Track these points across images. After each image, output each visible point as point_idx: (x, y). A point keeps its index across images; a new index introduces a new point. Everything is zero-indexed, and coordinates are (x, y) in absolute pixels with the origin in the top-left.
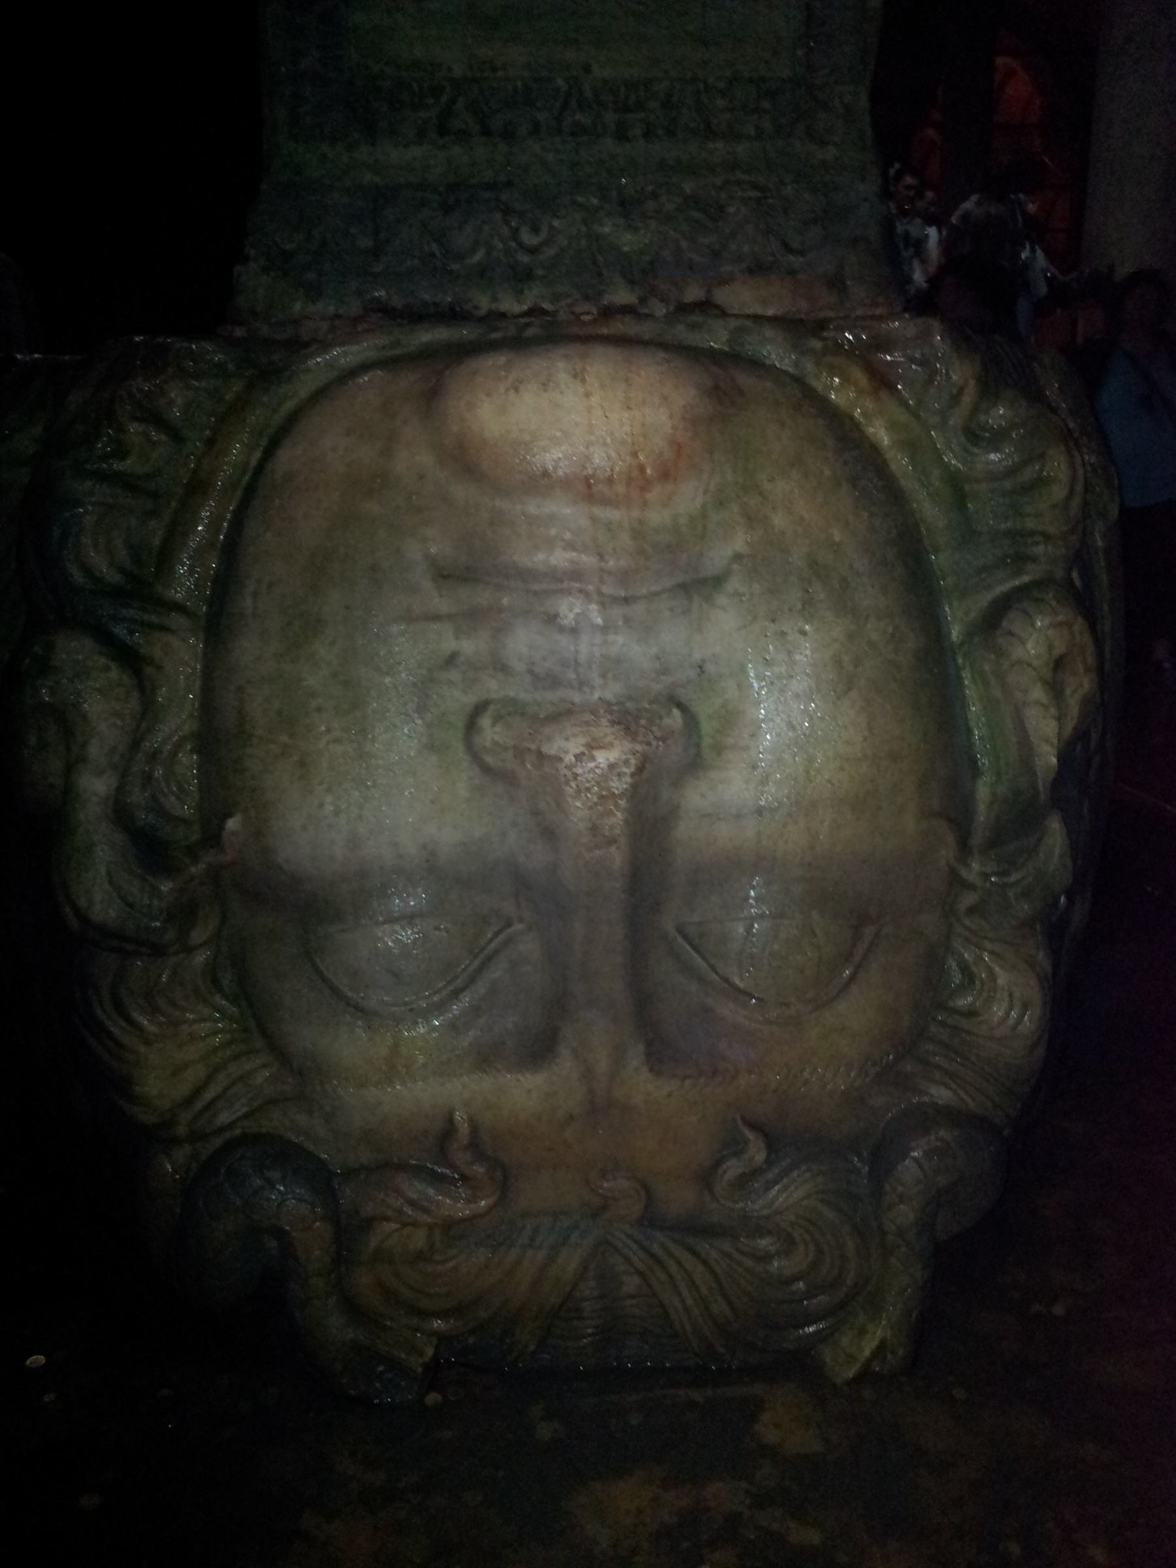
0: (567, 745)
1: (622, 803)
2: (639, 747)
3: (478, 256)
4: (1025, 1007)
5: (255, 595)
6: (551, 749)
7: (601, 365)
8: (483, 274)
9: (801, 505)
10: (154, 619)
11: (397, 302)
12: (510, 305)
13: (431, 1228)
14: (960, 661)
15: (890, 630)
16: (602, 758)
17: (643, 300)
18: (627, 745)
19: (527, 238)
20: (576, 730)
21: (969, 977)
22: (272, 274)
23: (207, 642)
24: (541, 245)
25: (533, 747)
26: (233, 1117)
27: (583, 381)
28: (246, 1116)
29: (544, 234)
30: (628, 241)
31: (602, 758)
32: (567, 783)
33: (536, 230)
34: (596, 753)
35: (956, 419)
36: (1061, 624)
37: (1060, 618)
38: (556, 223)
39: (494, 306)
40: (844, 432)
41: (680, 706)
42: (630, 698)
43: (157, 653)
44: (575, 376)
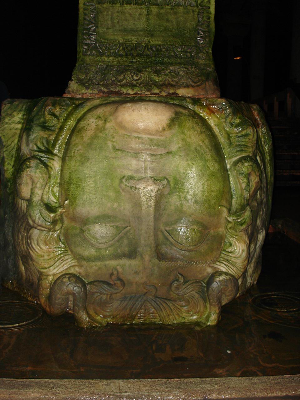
0: (141, 186)
1: (153, 198)
2: (157, 187)
4: (243, 251)
5: (74, 153)
6: (138, 186)
7: (151, 106)
8: (126, 85)
9: (195, 137)
10: (51, 157)
11: (106, 90)
12: (131, 92)
13: (107, 295)
14: (229, 173)
15: (212, 164)
16: (150, 188)
17: (160, 92)
18: (155, 186)
19: (135, 78)
21: (231, 245)
22: (78, 84)
24: (138, 79)
25: (134, 186)
26: (63, 270)
27: (147, 110)
28: (67, 269)
29: (139, 77)
30: (157, 79)
31: (150, 188)
32: (141, 193)
33: (137, 76)
34: (148, 187)
35: (228, 121)
36: (250, 165)
37: (250, 164)
38: (142, 75)
39: (127, 92)
40: (204, 122)
41: (167, 179)
42: (156, 177)
44: (146, 109)
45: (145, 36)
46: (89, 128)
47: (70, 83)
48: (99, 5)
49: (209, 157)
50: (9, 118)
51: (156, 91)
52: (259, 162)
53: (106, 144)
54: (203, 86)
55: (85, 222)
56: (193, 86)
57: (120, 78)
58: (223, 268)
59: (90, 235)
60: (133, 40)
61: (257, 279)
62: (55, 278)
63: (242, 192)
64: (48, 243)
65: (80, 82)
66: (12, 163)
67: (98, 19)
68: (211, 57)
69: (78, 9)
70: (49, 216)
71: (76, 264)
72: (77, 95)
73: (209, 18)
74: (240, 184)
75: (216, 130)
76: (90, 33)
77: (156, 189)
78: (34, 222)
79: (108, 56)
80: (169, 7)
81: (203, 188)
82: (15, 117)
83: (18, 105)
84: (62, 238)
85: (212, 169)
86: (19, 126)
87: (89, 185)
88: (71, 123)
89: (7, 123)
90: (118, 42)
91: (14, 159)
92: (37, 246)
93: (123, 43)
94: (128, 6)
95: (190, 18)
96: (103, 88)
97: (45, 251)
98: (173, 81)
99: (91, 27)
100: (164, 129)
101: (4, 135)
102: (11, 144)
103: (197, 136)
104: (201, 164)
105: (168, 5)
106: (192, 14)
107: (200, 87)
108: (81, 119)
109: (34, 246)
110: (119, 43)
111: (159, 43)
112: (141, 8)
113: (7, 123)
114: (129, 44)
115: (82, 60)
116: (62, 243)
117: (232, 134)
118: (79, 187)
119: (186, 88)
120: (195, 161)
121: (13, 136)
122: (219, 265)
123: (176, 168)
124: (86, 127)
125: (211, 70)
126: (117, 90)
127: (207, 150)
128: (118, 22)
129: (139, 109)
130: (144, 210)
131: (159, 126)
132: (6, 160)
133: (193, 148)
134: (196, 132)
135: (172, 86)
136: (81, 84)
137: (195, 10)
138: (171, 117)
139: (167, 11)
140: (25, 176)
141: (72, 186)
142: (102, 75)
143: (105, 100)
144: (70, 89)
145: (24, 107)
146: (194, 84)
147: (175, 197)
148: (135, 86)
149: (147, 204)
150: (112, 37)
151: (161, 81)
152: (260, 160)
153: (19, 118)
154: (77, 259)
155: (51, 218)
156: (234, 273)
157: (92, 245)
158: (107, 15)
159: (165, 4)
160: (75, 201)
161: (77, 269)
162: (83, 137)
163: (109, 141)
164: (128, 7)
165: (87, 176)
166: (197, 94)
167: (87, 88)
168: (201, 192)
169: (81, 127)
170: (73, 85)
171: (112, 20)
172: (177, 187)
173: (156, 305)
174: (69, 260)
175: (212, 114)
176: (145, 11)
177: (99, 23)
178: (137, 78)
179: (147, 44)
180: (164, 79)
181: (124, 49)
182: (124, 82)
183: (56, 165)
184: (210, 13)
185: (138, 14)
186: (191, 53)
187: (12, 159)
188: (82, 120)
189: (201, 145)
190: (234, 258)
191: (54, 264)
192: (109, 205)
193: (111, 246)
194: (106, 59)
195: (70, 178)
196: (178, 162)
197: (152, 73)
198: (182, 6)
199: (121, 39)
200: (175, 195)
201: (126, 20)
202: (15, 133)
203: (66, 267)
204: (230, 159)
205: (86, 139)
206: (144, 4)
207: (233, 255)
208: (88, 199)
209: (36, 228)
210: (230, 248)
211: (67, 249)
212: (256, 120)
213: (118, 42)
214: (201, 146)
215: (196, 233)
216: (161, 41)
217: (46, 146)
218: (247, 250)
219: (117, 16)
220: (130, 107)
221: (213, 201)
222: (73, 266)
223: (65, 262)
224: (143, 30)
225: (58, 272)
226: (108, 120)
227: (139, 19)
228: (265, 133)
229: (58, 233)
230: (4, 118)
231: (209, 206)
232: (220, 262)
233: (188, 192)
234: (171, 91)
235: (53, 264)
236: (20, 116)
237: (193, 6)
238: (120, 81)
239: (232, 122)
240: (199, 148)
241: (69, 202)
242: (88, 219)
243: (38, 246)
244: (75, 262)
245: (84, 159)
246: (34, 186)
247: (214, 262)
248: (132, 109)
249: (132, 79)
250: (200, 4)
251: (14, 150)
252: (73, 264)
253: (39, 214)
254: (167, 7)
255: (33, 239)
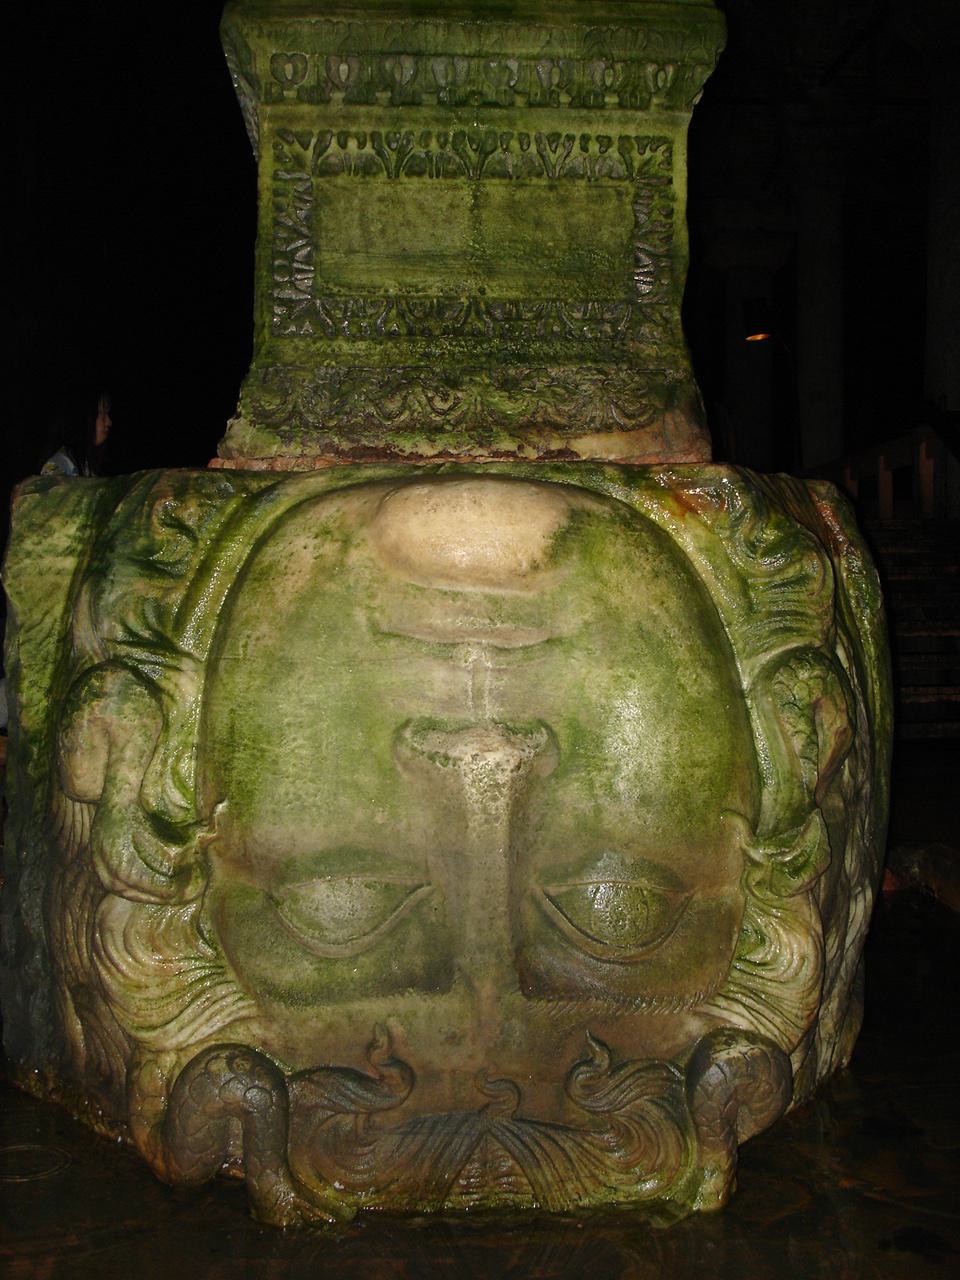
0: (464, 750)
1: (505, 791)
2: (516, 752)
3: (405, 416)
4: (803, 958)
5: (245, 646)
6: (453, 753)
8: (410, 429)
9: (635, 590)
10: (171, 662)
11: (345, 445)
12: (426, 450)
13: (356, 1114)
14: (749, 702)
16: (492, 758)
17: (520, 448)
18: (509, 750)
19: (439, 404)
20: (472, 739)
23: (206, 679)
24: (450, 409)
25: (442, 751)
26: (210, 1031)
27: (480, 505)
28: (222, 1030)
30: (509, 407)
31: (492, 758)
32: (465, 775)
33: (445, 400)
34: (487, 754)
35: (740, 535)
36: (816, 677)
37: (816, 673)
38: (460, 395)
39: (414, 450)
40: (661, 539)
41: (548, 727)
42: (512, 720)
45: (469, 273)
46: (294, 566)
47: (232, 426)
48: (320, 179)
49: (681, 652)
50: (35, 538)
51: (507, 444)
52: (845, 665)
53: (349, 615)
54: (655, 427)
55: (280, 872)
56: (623, 429)
57: (392, 406)
58: (740, 1019)
59: (299, 913)
60: (430, 287)
61: (849, 1049)
62: (185, 1061)
63: (792, 765)
64: (160, 942)
65: (265, 420)
66: (46, 682)
67: (319, 221)
68: (680, 334)
69: (254, 194)
70: (165, 854)
71: (253, 1011)
72: (255, 462)
73: (670, 214)
74: (787, 740)
75: (701, 564)
76: (295, 265)
77: (512, 761)
78: (114, 874)
79: (353, 339)
80: (544, 182)
81: (666, 755)
82: (56, 535)
83: (65, 497)
84: (206, 926)
85: (693, 691)
86: (70, 563)
87: (294, 751)
88: (236, 550)
89: (28, 554)
90: (382, 292)
91: (50, 668)
92: (125, 954)
93: (398, 297)
94: (415, 179)
95: (610, 215)
96: (336, 440)
97: (151, 971)
98: (559, 412)
99: (297, 249)
100: (535, 567)
101: (19, 593)
102: (42, 620)
103: (643, 587)
104: (656, 677)
105: (539, 175)
106: (614, 202)
107: (648, 429)
108: (269, 537)
109: (115, 955)
110: (387, 298)
111: (513, 294)
112: (456, 188)
113: (28, 554)
114: (419, 298)
115: (269, 352)
116: (206, 941)
117: (754, 576)
118: (262, 756)
119: (602, 435)
120: (637, 667)
121: (49, 595)
122: (725, 1009)
123: (575, 692)
124: (284, 563)
125: (680, 375)
126: (382, 445)
127: (674, 631)
128: (383, 232)
129: (453, 503)
130: (474, 829)
131: (519, 556)
132: (25, 671)
133: (628, 624)
134: (638, 574)
136: (268, 426)
137: (623, 190)
138: (556, 526)
139: (536, 194)
140: (85, 723)
141: (237, 755)
142: (331, 400)
143: (345, 477)
144: (232, 444)
145: (85, 500)
146: (627, 421)
147: (576, 785)
148: (439, 429)
149: (485, 810)
150: (365, 279)
152: (848, 658)
153: (69, 537)
154: (255, 996)
155: (169, 860)
156: (777, 1033)
157: (307, 949)
158: (346, 210)
159: (529, 173)
160: (249, 804)
161: (256, 1029)
162: (274, 594)
163: (358, 609)
164: (414, 183)
165: (286, 720)
166: (637, 453)
167: (287, 439)
168: (659, 769)
169: (266, 564)
170: (241, 431)
171: (364, 224)
172: (582, 751)
173: (521, 1147)
174: (230, 1000)
175: (687, 515)
176: (466, 196)
177: (323, 234)
178: (446, 406)
179: (474, 298)
180: (532, 408)
181: (401, 315)
182: (402, 418)
183: (187, 687)
184: (673, 199)
185: (444, 206)
186: (614, 323)
187: (45, 667)
188: (271, 542)
189: (658, 616)
190: (775, 984)
191: (181, 1012)
192: (360, 815)
193: (368, 950)
194: (346, 347)
195: (232, 727)
196: (583, 670)
197: (492, 389)
198: (582, 177)
199: (392, 282)
200: (577, 780)
201: (408, 224)
202: (56, 586)
203: (218, 1022)
204: (749, 656)
205: (283, 602)
206: (463, 174)
207: (769, 975)
208: (291, 796)
209: (120, 894)
210: (760, 949)
211: (225, 962)
212: (828, 529)
213: (382, 292)
214: (655, 619)
215: (645, 903)
216: (517, 289)
217: (156, 626)
218: (817, 957)
219: (380, 212)
220: (424, 496)
221: (701, 796)
222: (243, 1020)
223: (217, 1006)
224: (462, 254)
225: (192, 1040)
226: (355, 541)
227: (447, 221)
228: (860, 572)
229: (192, 908)
230: (21, 538)
231: (689, 812)
232: (727, 998)
233: (617, 768)
234: (556, 445)
235: (177, 1012)
236: (72, 530)
237: (620, 178)
238: (389, 417)
239: (752, 538)
240: (648, 625)
241: (229, 807)
242: (291, 863)
243: (129, 953)
244: (249, 1006)
245: (280, 666)
246: (114, 757)
247: (709, 999)
248: (432, 502)
249: (429, 409)
250: (640, 171)
251: (53, 639)
252: (244, 1013)
253: (132, 849)
254: (535, 181)
255: (111, 931)
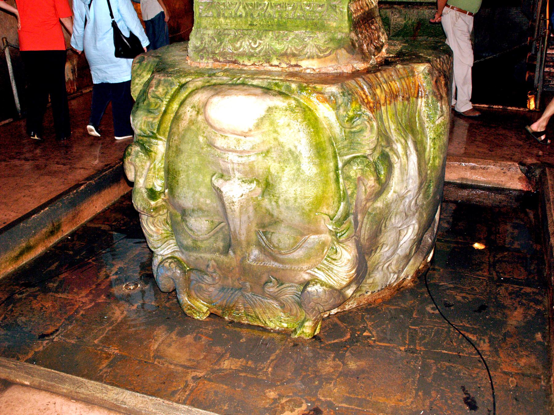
17: (280, 63)
19: (253, 45)
24: (258, 47)
33: (255, 44)
37: (359, 168)
38: (261, 42)
43: (155, 150)
50: (139, 79)
51: (275, 62)
56: (319, 57)
57: (238, 45)
58: (321, 276)
59: (187, 226)
64: (156, 225)
71: (178, 250)
89: (137, 84)
98: (296, 49)
109: (145, 226)
126: (234, 60)
133: (286, 149)
135: (294, 55)
142: (218, 41)
148: (252, 55)
151: (282, 50)
161: (180, 254)
174: (173, 245)
181: (244, 8)
203: (170, 251)
205: (181, 130)
222: (177, 251)
233: (279, 197)
234: (293, 63)
238: (236, 49)
240: (293, 149)
252: (176, 249)
